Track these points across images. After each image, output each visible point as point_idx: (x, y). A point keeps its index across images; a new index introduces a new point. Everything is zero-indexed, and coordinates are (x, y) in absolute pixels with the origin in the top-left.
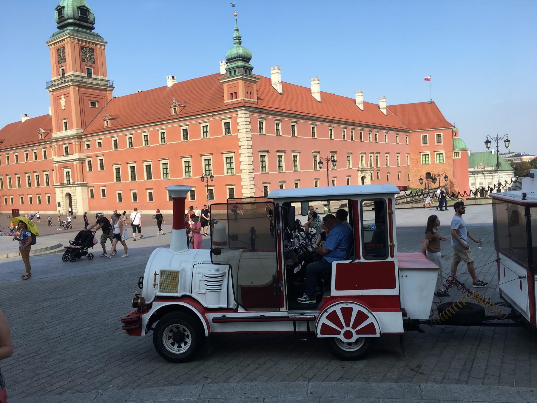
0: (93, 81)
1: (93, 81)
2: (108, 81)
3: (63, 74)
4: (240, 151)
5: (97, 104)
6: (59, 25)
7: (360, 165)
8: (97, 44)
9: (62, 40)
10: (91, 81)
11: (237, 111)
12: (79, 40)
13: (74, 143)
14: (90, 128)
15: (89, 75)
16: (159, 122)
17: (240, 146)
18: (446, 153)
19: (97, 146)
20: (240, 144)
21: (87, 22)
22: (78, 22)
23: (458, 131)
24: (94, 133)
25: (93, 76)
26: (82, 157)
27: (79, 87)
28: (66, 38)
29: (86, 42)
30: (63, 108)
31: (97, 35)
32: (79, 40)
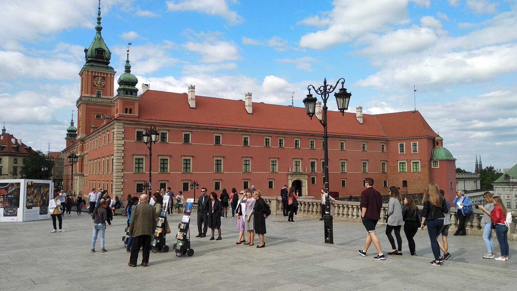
0: (101, 100)
1: (101, 100)
7: (290, 170)
8: (107, 74)
10: (98, 100)
12: (92, 72)
15: (99, 95)
18: (421, 162)
21: (103, 59)
22: (94, 59)
23: (442, 140)
25: (102, 97)
26: (83, 154)
29: (98, 73)
31: (108, 67)
32: (92, 72)
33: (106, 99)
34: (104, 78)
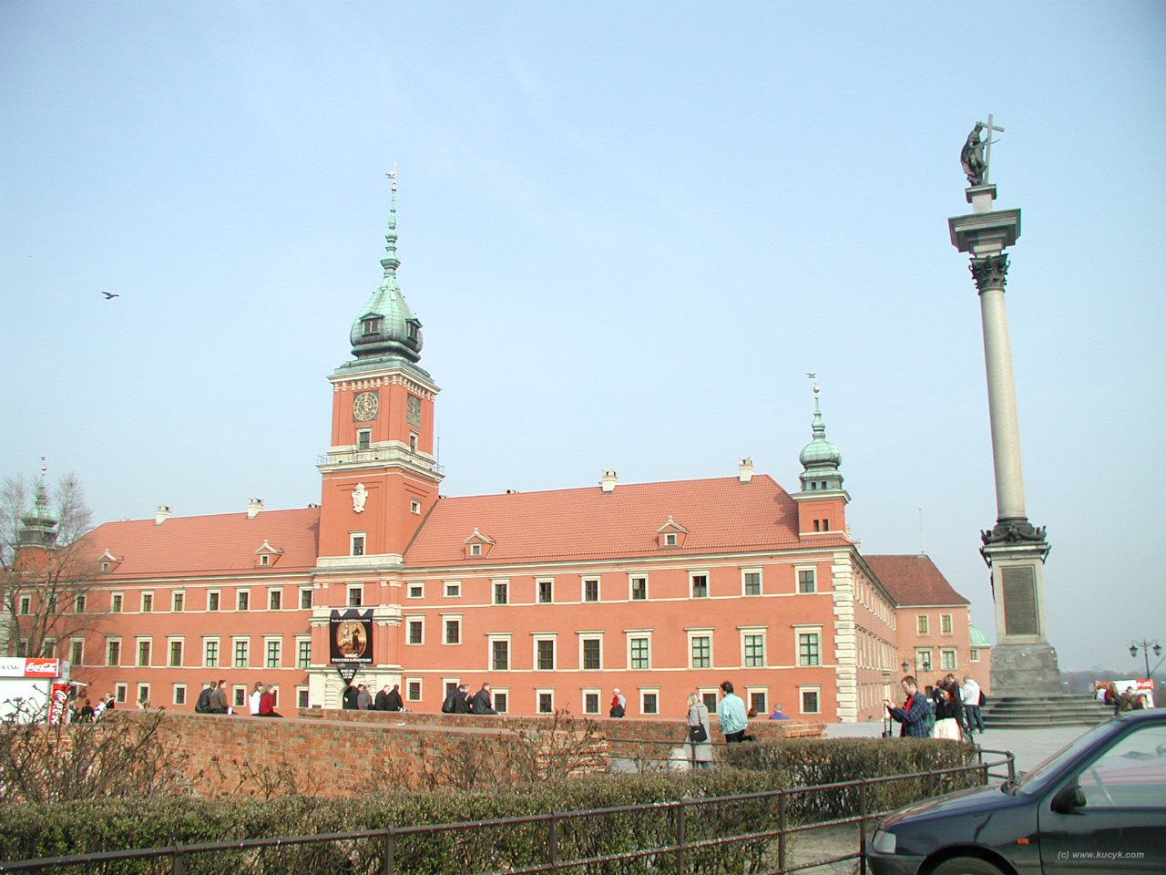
2: (433, 463)
3: (365, 443)
4: (837, 624)
5: (418, 506)
6: (359, 347)
8: (427, 391)
9: (375, 379)
11: (832, 553)
13: (384, 584)
14: (415, 553)
15: (413, 447)
16: (637, 558)
17: (837, 616)
19: (445, 595)
20: (836, 611)
22: (404, 347)
24: (443, 566)
26: (399, 613)
27: (404, 471)
28: (390, 377)
30: (358, 509)
33: (428, 460)
34: (419, 399)
